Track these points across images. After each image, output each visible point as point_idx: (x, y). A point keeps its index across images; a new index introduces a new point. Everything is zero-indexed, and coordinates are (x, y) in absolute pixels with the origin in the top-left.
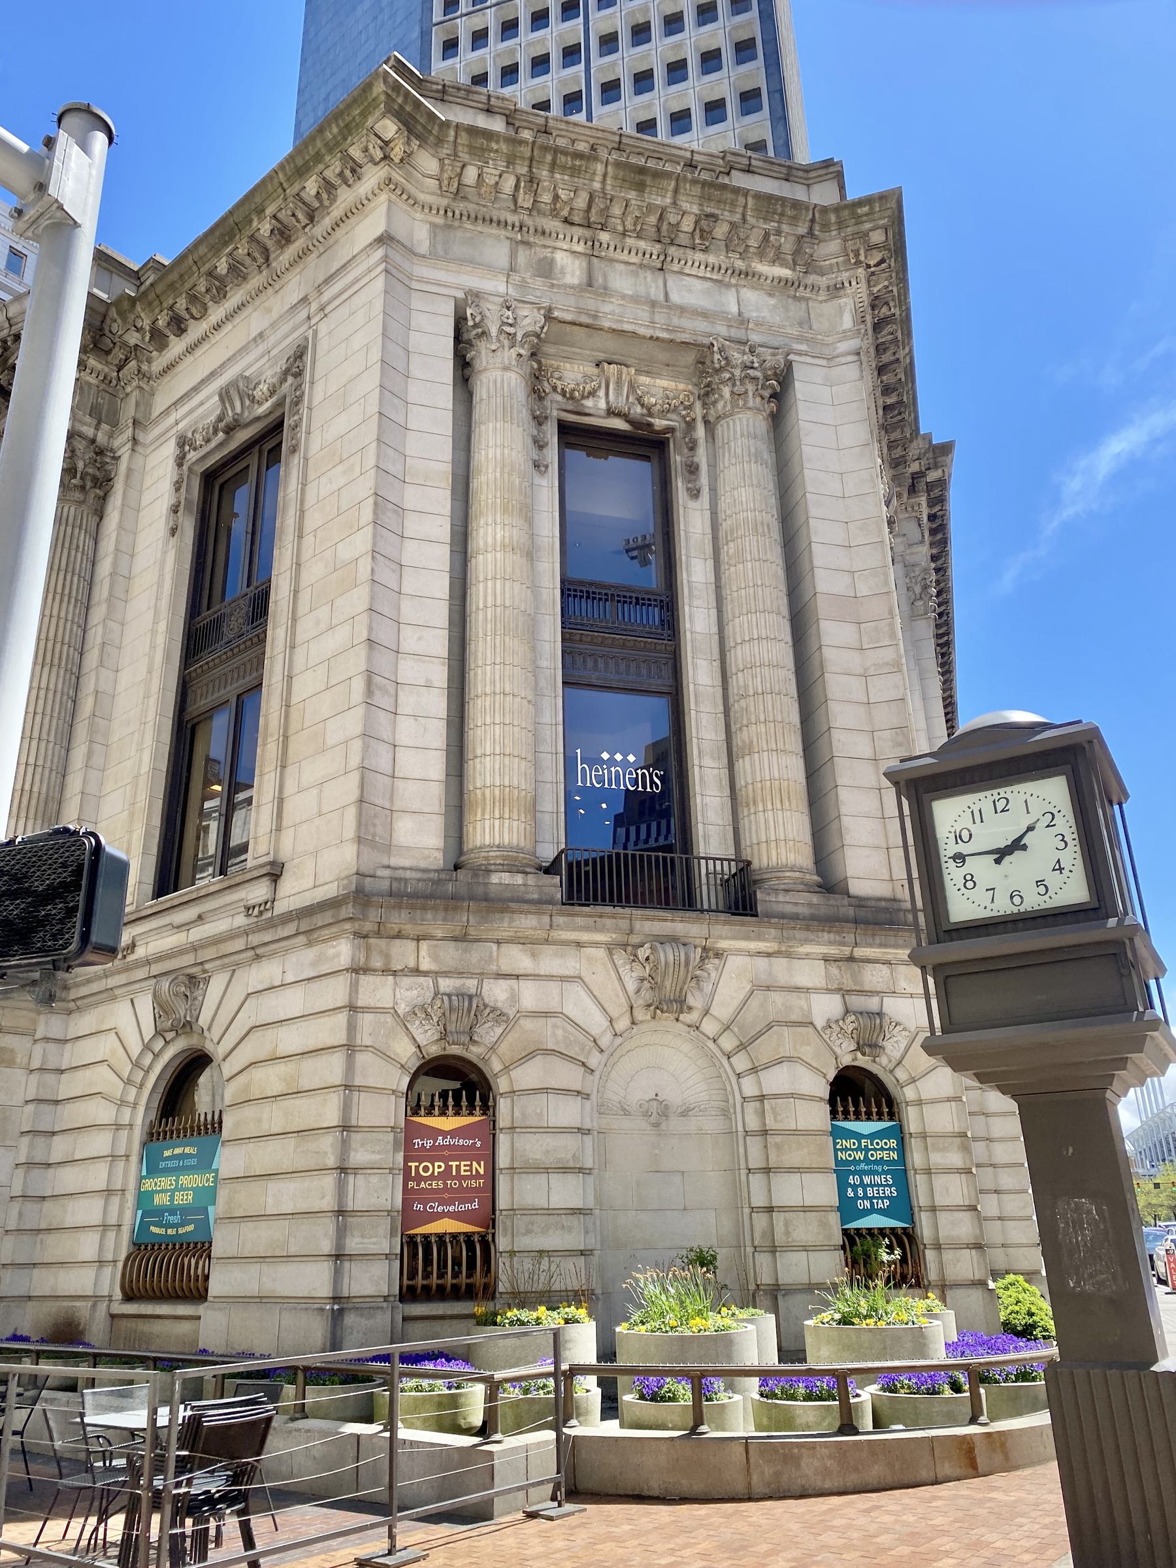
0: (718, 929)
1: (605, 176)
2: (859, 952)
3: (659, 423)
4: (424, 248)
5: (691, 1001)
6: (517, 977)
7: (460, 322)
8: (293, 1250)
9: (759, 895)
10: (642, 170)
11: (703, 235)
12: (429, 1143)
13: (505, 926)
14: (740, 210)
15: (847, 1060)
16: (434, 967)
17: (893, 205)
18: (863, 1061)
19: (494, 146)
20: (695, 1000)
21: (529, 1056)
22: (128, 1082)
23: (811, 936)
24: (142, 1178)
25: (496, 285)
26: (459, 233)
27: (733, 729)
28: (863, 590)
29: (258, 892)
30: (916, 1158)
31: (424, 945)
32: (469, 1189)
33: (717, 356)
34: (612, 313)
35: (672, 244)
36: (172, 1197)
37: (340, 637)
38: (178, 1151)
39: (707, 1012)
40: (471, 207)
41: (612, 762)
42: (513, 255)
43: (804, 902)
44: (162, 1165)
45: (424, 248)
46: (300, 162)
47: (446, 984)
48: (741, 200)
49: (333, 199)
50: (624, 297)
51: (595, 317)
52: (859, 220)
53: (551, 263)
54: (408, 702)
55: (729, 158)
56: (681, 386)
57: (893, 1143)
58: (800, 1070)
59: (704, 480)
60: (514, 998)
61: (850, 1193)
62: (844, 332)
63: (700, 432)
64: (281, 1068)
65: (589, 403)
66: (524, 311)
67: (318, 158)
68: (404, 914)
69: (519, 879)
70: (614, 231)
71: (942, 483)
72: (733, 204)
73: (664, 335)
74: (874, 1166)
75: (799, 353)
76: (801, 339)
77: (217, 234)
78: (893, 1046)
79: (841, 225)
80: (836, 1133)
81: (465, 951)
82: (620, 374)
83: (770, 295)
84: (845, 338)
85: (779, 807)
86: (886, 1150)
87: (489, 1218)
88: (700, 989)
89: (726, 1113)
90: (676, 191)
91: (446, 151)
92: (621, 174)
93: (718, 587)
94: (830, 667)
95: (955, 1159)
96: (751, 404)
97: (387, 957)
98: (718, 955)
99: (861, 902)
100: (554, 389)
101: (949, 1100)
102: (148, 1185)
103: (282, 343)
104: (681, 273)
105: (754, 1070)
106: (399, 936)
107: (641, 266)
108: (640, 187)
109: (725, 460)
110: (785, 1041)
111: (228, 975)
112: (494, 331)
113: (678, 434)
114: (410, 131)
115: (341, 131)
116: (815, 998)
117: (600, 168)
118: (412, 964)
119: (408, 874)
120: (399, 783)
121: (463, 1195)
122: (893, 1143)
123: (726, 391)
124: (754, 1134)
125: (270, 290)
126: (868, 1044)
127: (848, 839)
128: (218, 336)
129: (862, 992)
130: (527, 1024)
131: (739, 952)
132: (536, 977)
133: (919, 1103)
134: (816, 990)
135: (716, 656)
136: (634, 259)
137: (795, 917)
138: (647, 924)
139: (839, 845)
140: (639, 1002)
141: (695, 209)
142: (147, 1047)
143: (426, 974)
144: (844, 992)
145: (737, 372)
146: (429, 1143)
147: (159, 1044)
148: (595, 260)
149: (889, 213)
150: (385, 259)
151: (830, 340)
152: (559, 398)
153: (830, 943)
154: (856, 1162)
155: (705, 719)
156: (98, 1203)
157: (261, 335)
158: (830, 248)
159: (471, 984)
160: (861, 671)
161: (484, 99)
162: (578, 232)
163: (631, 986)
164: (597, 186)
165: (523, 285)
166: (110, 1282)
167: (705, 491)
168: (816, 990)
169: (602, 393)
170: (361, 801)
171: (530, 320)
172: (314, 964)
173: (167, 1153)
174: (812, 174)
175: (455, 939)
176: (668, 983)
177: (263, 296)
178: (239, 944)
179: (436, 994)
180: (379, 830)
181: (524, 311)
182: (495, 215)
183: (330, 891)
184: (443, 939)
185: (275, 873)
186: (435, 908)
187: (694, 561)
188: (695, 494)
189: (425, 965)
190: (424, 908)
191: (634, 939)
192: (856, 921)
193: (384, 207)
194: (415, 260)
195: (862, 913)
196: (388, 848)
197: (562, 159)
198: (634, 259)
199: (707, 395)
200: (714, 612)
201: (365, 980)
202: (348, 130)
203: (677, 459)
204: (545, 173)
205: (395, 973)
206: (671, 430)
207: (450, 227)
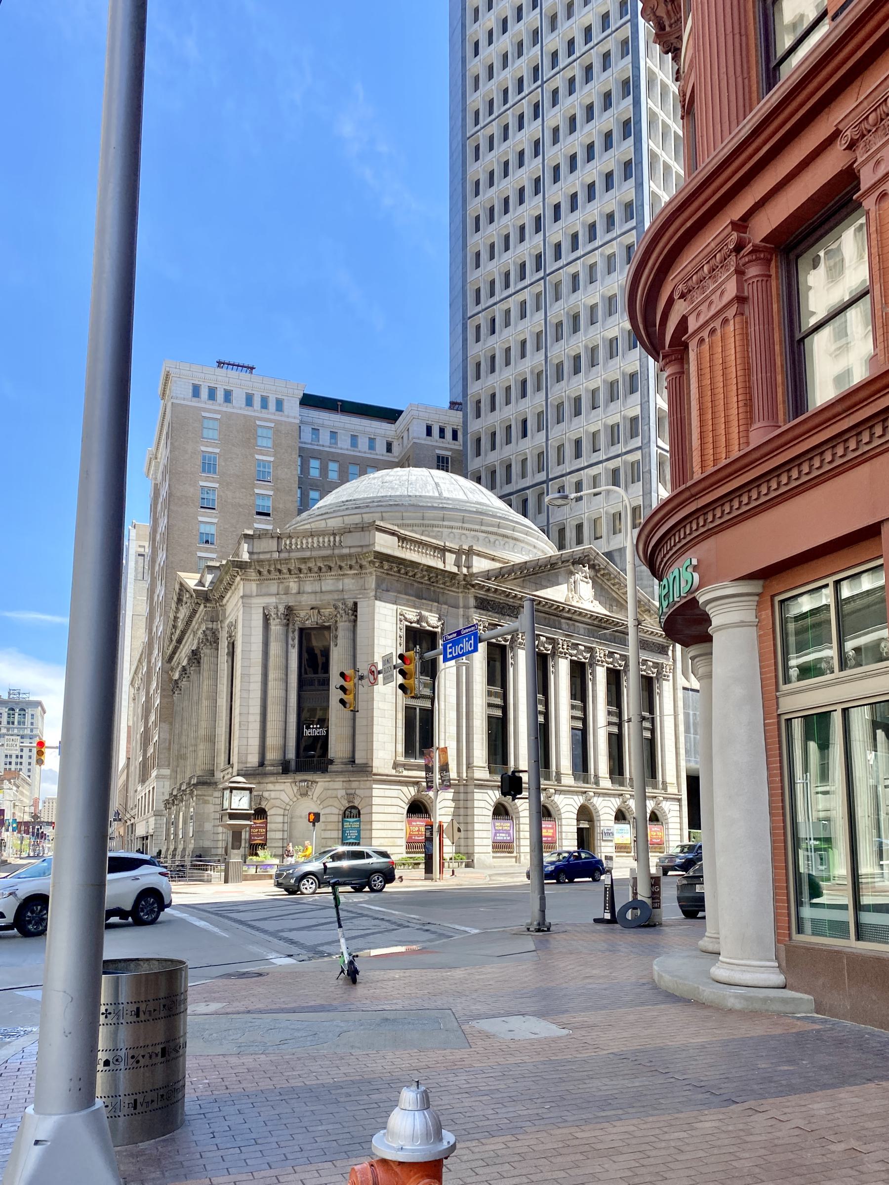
3: (326, 624)
7: (264, 613)
10: (304, 559)
25: (273, 600)
41: (313, 728)
42: (278, 587)
45: (254, 594)
53: (289, 586)
54: (251, 727)
75: (360, 598)
76: (360, 594)
83: (353, 579)
108: (305, 563)
117: (293, 561)
162: (294, 576)
197: (282, 562)
207: (261, 584)
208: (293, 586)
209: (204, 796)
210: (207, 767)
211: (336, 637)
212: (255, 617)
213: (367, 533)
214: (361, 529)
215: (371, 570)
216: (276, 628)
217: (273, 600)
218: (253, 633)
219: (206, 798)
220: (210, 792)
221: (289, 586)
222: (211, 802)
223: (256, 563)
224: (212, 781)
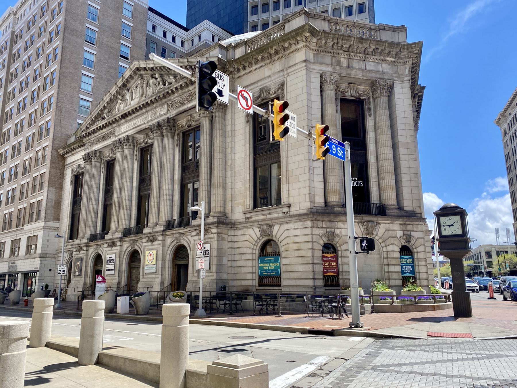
0: (379, 219)
1: (354, 41)
2: (407, 223)
3: (362, 98)
4: (312, 61)
5: (374, 233)
6: (341, 228)
8: (303, 278)
9: (387, 211)
10: (362, 39)
11: (374, 52)
12: (326, 259)
13: (338, 219)
14: (384, 46)
15: (403, 244)
16: (326, 227)
17: (421, 45)
18: (406, 244)
19: (330, 36)
20: (375, 233)
21: (344, 244)
22: (254, 245)
23: (397, 220)
24: (259, 264)
25: (328, 69)
26: (320, 55)
27: (380, 173)
28: (409, 141)
29: (286, 210)
30: (416, 263)
31: (323, 222)
32: (334, 268)
33: (377, 84)
34: (354, 74)
35: (367, 54)
36: (269, 268)
37: (301, 157)
38: (268, 259)
39: (377, 235)
40: (323, 49)
42: (332, 60)
43: (395, 212)
44: (265, 261)
45: (312, 61)
46: (284, 38)
47: (328, 230)
48: (385, 44)
49: (291, 47)
50: (357, 69)
51: (350, 75)
52: (412, 48)
55: (380, 27)
56: (367, 88)
57: (411, 260)
58: (395, 246)
59: (372, 112)
60: (341, 233)
61: (403, 269)
62: (406, 75)
63: (371, 99)
64: (296, 245)
65: (346, 94)
66: (335, 75)
67: (289, 39)
68: (320, 216)
69: (340, 209)
70: (355, 52)
71: (422, 96)
72: (383, 45)
73: (365, 78)
74: (407, 264)
75: (396, 80)
76: (396, 77)
77: (259, 50)
78: (413, 241)
79: (408, 49)
80: (401, 258)
81: (331, 223)
82: (354, 86)
83: (389, 65)
84: (406, 77)
85: (390, 191)
86: (410, 261)
87: (337, 272)
88: (375, 230)
89: (379, 254)
90: (370, 43)
91: (319, 38)
92: (358, 40)
93: (376, 138)
94: (401, 159)
95: (424, 263)
96: (385, 95)
97: (317, 225)
98: (379, 224)
99: (407, 212)
100: (339, 91)
101: (423, 252)
102: (261, 265)
103: (277, 80)
104: (369, 61)
105: (386, 246)
106: (319, 221)
107: (360, 60)
108: (362, 43)
109: (378, 109)
110: (392, 240)
111: (279, 226)
112: (328, 81)
113: (367, 100)
114: (312, 35)
115: (296, 34)
116: (397, 232)
117: (353, 39)
119: (319, 208)
120: (315, 189)
121: (333, 269)
122: (411, 260)
123: (379, 91)
124: (385, 258)
125: (271, 64)
126: (408, 241)
127: (404, 198)
128: (255, 72)
129: (407, 231)
130: (343, 237)
131: (383, 223)
132: (344, 228)
133: (417, 252)
134: (398, 230)
135: (375, 155)
136: (358, 58)
137: (394, 216)
138: (366, 218)
139: (402, 199)
140: (364, 233)
141: (374, 47)
142: (258, 238)
143: (324, 228)
144: (403, 231)
145: (382, 87)
146: (326, 259)
147: (261, 238)
148: (350, 60)
149: (419, 47)
150: (306, 66)
151: (403, 76)
152: (340, 93)
153: (401, 221)
154: (404, 263)
155: (373, 170)
156: (251, 268)
157: (270, 76)
158: (404, 54)
159: (333, 230)
160: (408, 160)
161: (324, 17)
162: (346, 53)
163: (362, 230)
164: (352, 43)
165: (334, 69)
166: (256, 283)
167: (373, 114)
168: (398, 230)
169: (349, 91)
170: (310, 194)
171: (336, 77)
172: (302, 225)
173: (265, 259)
174: (399, 30)
175: (329, 221)
176: (370, 230)
177: (269, 65)
178: (283, 220)
179: (327, 232)
180: (313, 199)
181: (335, 75)
182: (328, 50)
183: (304, 211)
184: (327, 221)
185: (289, 206)
186: (326, 215)
187: (370, 132)
188: (370, 115)
189: (324, 226)
190: (324, 215)
191: (363, 221)
192: (406, 216)
193: (305, 51)
194: (311, 64)
195: (407, 214)
196: (314, 203)
197: (345, 38)
198: (358, 58)
199: (374, 91)
200: (375, 145)
201: (314, 229)
202: (297, 34)
203: (366, 107)
204: (341, 41)
205: (319, 228)
206: (365, 99)
207: (317, 54)
208: (344, 62)
209: (222, 233)
210: (221, 209)
211: (370, 109)
212: (313, 80)
213: (396, 34)
214: (393, 29)
215: (407, 60)
216: (330, 93)
217: (328, 69)
218: (313, 93)
219: (224, 236)
220: (225, 231)
221: (340, 61)
222: (226, 239)
223: (323, 34)
224: (227, 222)
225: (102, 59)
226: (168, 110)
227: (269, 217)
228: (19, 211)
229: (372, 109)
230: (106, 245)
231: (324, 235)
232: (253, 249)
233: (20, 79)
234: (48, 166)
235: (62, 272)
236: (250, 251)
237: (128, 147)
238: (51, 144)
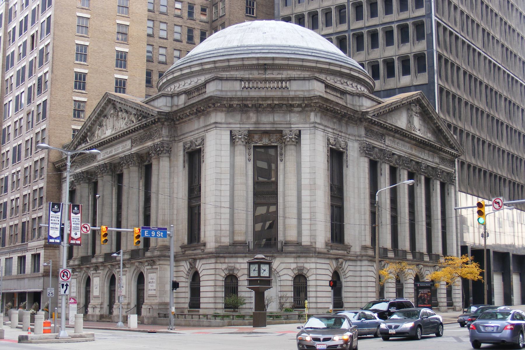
118: (224, 262)
130: (242, 270)
185: (204, 245)
196: (220, 242)
211: (281, 155)
225: (96, 49)
226: (132, 146)
227: (195, 252)
228: (24, 223)
229: (284, 153)
230: (92, 269)
231: (226, 269)
232: (186, 278)
233: (16, 68)
234: (45, 180)
235: (51, 294)
236: (184, 280)
237: (106, 174)
238: (47, 157)
